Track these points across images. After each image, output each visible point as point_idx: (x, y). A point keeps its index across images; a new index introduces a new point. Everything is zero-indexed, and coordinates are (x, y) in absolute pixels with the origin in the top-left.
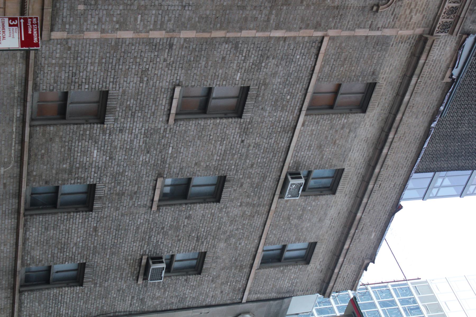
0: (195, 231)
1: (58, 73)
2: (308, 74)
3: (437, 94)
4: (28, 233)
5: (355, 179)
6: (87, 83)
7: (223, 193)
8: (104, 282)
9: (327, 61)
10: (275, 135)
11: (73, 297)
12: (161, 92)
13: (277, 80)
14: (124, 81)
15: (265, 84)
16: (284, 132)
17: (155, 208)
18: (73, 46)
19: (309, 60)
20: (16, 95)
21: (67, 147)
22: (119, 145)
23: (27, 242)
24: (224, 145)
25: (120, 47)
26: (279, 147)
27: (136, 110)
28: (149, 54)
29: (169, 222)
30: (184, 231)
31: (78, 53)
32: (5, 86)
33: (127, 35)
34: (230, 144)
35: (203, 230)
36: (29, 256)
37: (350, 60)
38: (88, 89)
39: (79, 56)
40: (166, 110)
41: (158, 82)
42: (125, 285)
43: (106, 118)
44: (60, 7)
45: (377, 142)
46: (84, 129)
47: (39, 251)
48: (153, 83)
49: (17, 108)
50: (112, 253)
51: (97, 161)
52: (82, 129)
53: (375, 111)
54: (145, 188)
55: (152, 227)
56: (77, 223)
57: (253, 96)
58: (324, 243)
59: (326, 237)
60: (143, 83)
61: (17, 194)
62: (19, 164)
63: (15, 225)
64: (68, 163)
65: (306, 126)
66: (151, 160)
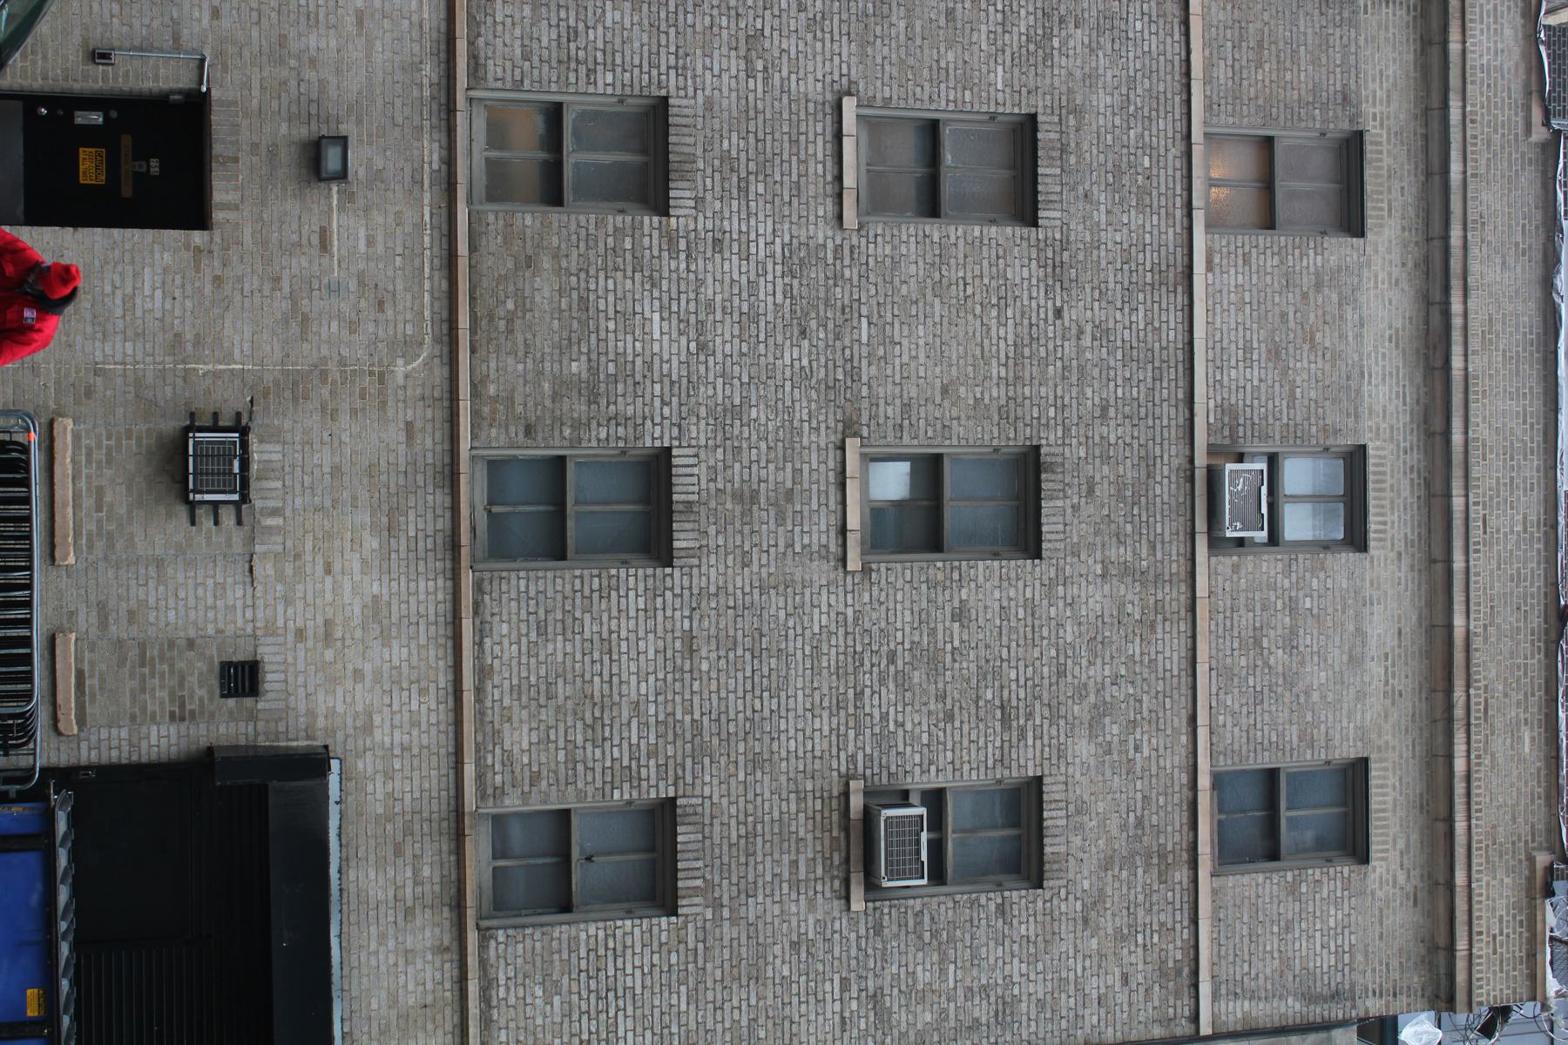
0: (989, 677)
1: (532, 25)
2: (1177, 86)
3: (1528, 180)
4: (487, 641)
5: (1405, 486)
6: (609, 67)
7: (1044, 520)
8: (743, 896)
9: (1215, 45)
10: (1141, 296)
11: (653, 965)
12: (807, 113)
13: (1102, 100)
14: (705, 68)
15: (1077, 111)
16: (1164, 289)
17: (854, 563)
19: (1169, 39)
20: (427, 93)
21: (575, 295)
22: (718, 298)
23: (489, 688)
24: (1010, 322)
26: (1164, 344)
27: (749, 173)
29: (907, 629)
30: (957, 673)
32: (397, 58)
34: (1026, 322)
35: (1013, 675)
36: (498, 751)
37: (1273, 47)
38: (613, 85)
40: (829, 178)
41: (793, 77)
42: (811, 921)
43: (672, 194)
45: (1427, 348)
46: (616, 229)
47: (525, 729)
48: (782, 79)
49: (432, 140)
50: (755, 762)
51: (666, 357)
52: (610, 230)
53: (1386, 232)
54: (815, 476)
55: (859, 648)
56: (632, 613)
57: (1053, 149)
58: (1389, 765)
59: (1389, 737)
60: (755, 77)
61: (447, 469)
62: (446, 350)
63: (449, 606)
64: (584, 358)
65: (1217, 270)
66: (815, 364)
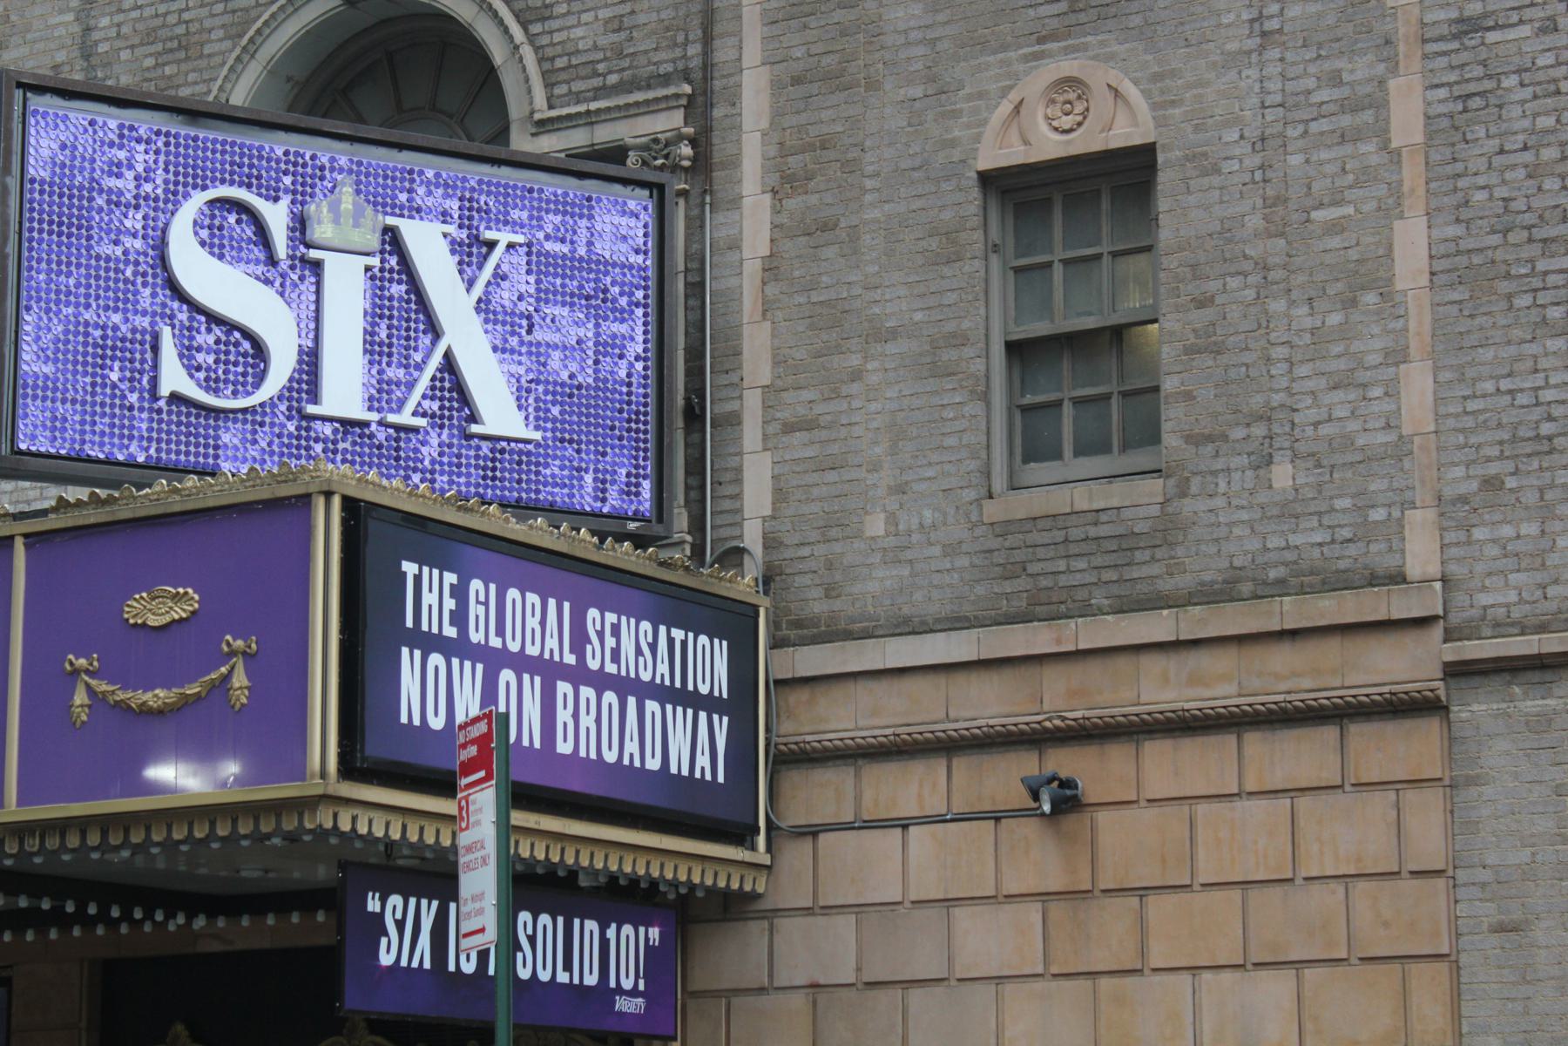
18: (1477, 470)
25: (1476, 260)
28: (1516, 111)
31: (1514, 439)
33: (1411, 245)
39: (1531, 434)
44: (1286, 564)
